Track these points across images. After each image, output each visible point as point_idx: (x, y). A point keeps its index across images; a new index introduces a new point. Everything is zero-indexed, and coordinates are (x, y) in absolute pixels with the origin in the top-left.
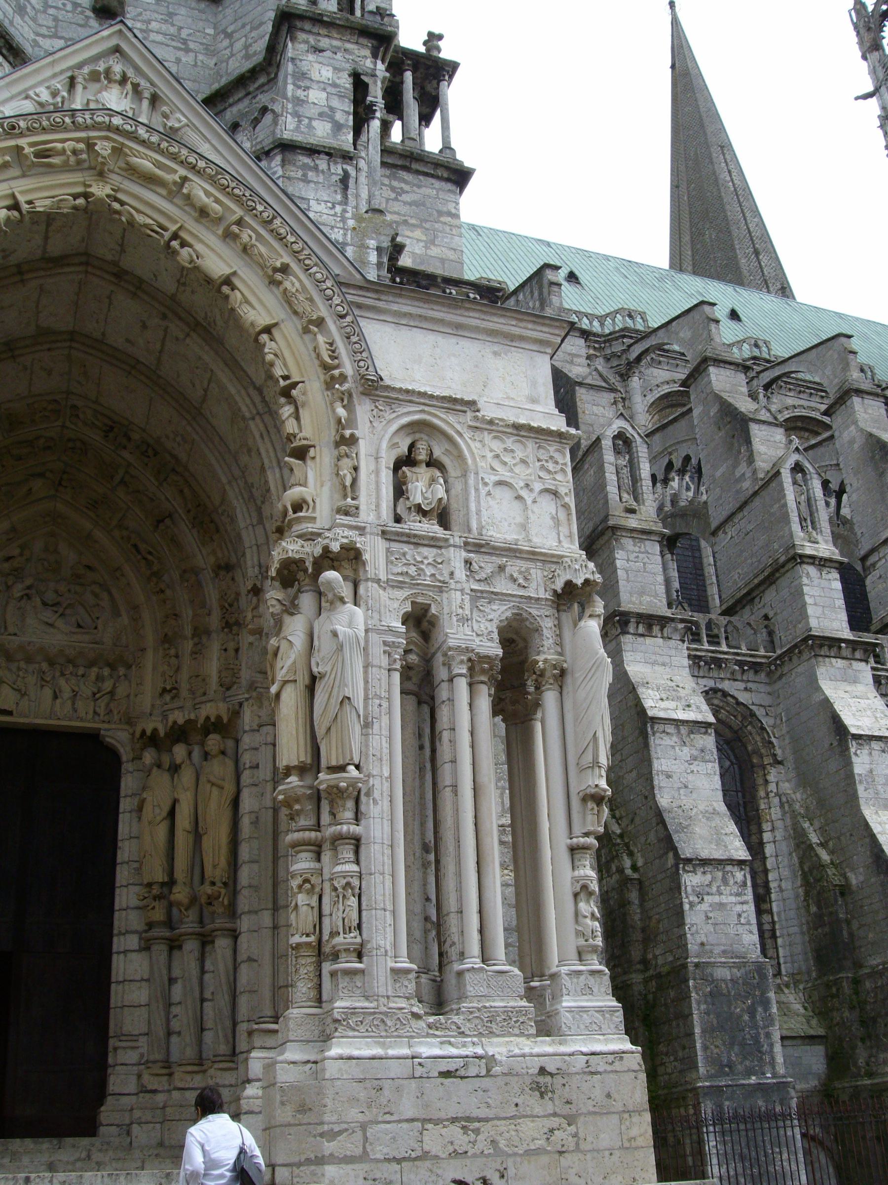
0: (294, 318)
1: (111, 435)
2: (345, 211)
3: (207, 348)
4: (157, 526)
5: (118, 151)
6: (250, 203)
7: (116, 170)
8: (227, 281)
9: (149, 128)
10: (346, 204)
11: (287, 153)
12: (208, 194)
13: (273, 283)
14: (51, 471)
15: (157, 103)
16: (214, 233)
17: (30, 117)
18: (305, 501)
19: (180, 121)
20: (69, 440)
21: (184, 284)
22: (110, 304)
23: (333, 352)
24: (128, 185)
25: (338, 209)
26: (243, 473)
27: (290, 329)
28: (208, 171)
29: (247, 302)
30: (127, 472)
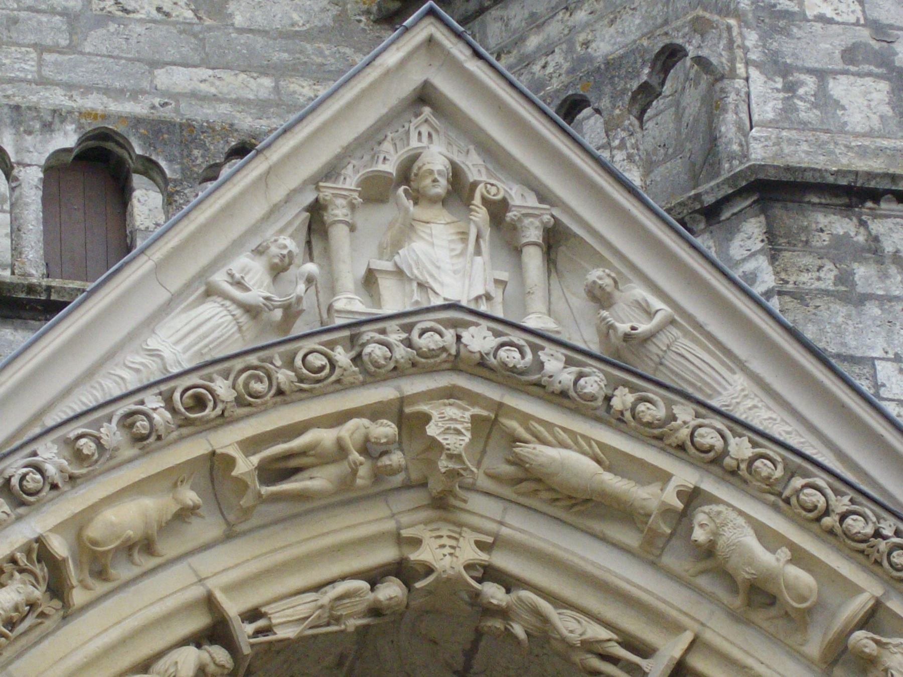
5: (487, 428)
7: (484, 482)
9: (575, 354)
11: (778, 211)
12: (763, 533)
15: (563, 253)
17: (239, 364)
19: (650, 314)
24: (524, 527)
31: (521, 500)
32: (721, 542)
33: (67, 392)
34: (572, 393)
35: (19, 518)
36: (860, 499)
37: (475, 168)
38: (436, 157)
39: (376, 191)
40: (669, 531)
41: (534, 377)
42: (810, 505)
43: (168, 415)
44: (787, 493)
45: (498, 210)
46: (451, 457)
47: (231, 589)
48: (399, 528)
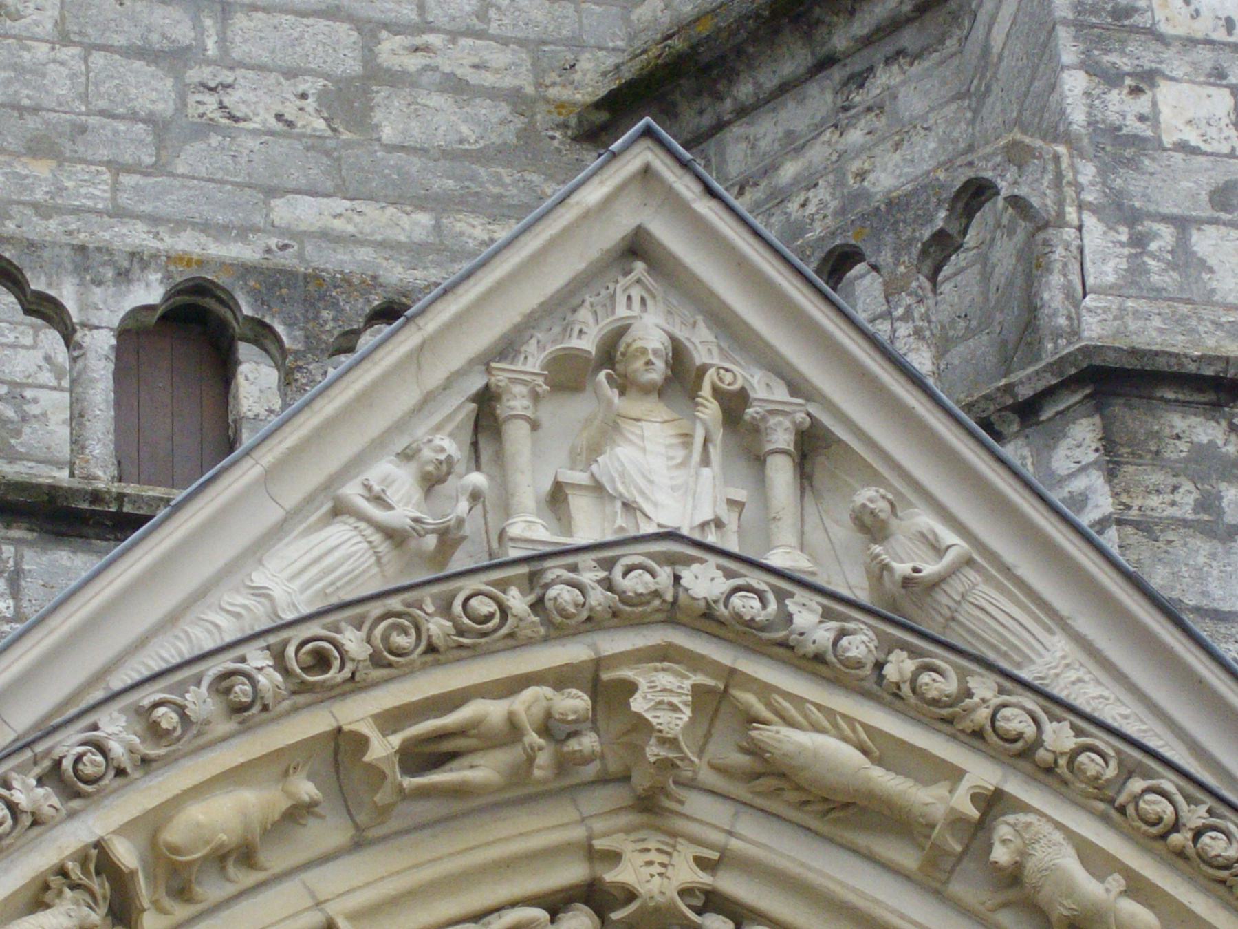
5: (712, 703)
7: (707, 777)
9: (836, 603)
11: (1117, 408)
12: (1089, 854)
15: (821, 466)
17: (376, 609)
19: (939, 550)
24: (757, 838)
31: (759, 802)
32: (1030, 865)
33: (141, 643)
34: (830, 657)
35: (72, 815)
36: (1222, 809)
37: (704, 347)
38: (651, 330)
39: (568, 375)
40: (958, 848)
41: (780, 635)
43: (278, 677)
44: (1121, 799)
45: (734, 405)
46: (663, 741)
48: (590, 838)
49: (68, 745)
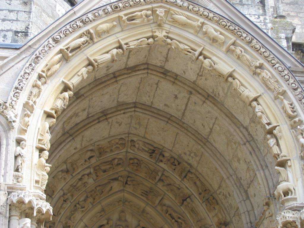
0: (269, 92)
1: (154, 155)
2: (265, 19)
3: (215, 108)
4: (183, 203)
5: (167, 12)
6: (239, 33)
8: (231, 75)
10: (265, 15)
12: (216, 30)
13: (255, 73)
14: (121, 177)
16: (221, 51)
18: (289, 190)
20: (130, 159)
21: (201, 76)
22: (157, 87)
23: (293, 108)
24: (173, 29)
25: (262, 18)
26: (235, 172)
27: (267, 99)
28: (215, 18)
29: (242, 85)
30: (163, 174)
31: (174, 25)
32: (208, 31)
33: (94, 6)
34: (182, 6)
35: (85, 26)
36: (232, 23)
40: (199, 29)
41: (175, 4)
42: (223, 25)
43: (111, 9)
44: (219, 22)
46: (161, 17)
47: (122, 39)
48: (152, 30)
49: (84, 18)
